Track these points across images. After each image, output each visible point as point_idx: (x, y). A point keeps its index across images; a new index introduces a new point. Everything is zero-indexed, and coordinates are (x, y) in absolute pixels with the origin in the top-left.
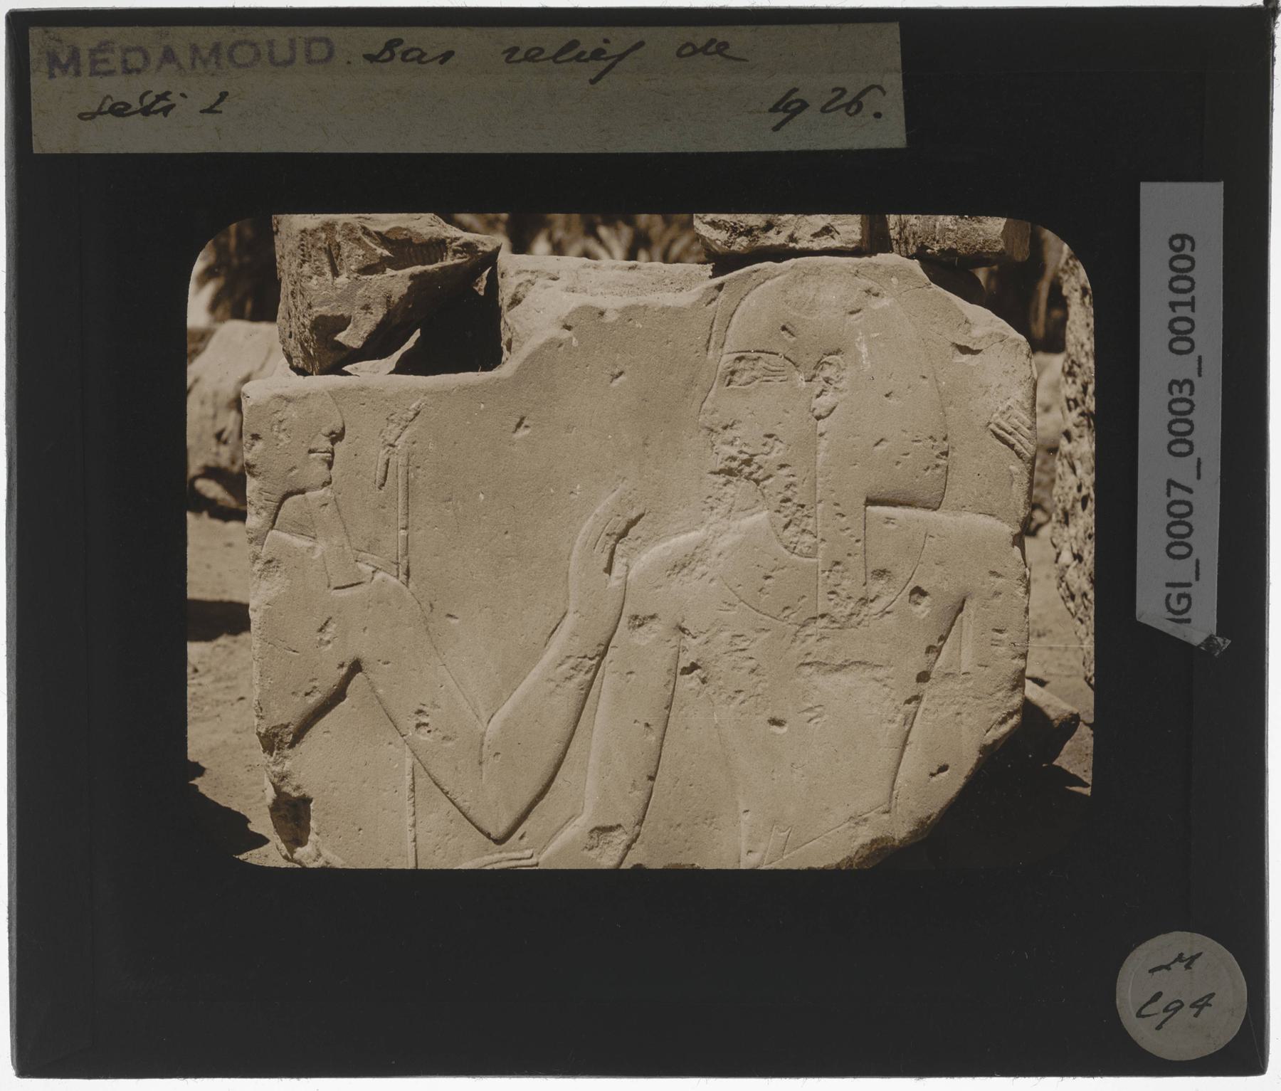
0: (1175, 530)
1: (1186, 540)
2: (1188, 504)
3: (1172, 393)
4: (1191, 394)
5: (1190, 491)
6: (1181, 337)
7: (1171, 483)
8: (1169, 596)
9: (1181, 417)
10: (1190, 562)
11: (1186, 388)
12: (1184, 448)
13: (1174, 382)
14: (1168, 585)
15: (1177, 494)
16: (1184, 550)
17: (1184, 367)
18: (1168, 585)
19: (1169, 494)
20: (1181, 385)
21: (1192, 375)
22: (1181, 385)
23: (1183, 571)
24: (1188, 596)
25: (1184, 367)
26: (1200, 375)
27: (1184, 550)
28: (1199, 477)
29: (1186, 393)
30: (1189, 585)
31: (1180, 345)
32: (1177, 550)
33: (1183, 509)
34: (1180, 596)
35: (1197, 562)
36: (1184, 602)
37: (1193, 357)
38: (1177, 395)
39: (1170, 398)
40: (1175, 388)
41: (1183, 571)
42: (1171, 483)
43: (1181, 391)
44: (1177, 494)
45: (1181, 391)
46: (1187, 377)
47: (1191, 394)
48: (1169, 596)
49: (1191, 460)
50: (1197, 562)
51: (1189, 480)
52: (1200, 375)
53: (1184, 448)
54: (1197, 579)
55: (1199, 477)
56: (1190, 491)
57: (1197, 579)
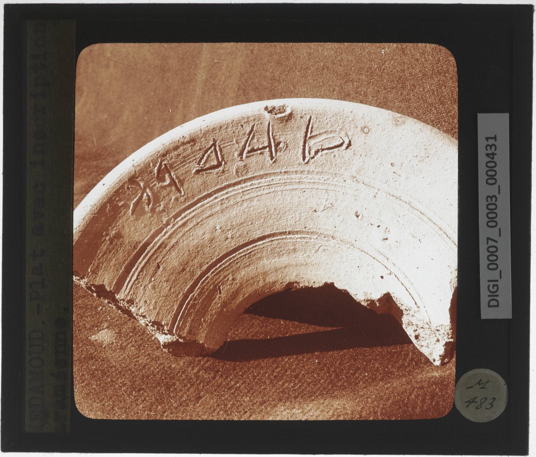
0: (491, 258)
1: (496, 262)
2: (496, 247)
3: (487, 201)
4: (496, 201)
5: (496, 242)
6: (492, 178)
7: (488, 239)
8: (489, 286)
9: (492, 211)
10: (497, 272)
11: (494, 199)
12: (493, 224)
13: (488, 197)
14: (489, 281)
15: (491, 243)
16: (495, 266)
17: (493, 190)
18: (489, 281)
19: (488, 244)
20: (491, 198)
21: (496, 194)
22: (491, 198)
23: (495, 275)
24: (497, 285)
25: (493, 190)
26: (499, 193)
27: (495, 266)
28: (500, 236)
29: (493, 201)
30: (497, 281)
31: (490, 181)
32: (491, 267)
33: (493, 249)
34: (494, 286)
35: (500, 271)
36: (496, 288)
37: (496, 186)
38: (490, 202)
39: (488, 203)
40: (489, 199)
41: (495, 275)
42: (488, 239)
43: (491, 200)
44: (491, 243)
45: (491, 200)
46: (494, 194)
47: (496, 201)
48: (489, 286)
49: (496, 229)
50: (500, 271)
51: (495, 237)
52: (499, 193)
53: (493, 224)
54: (501, 278)
55: (500, 236)
56: (496, 242)
57: (501, 278)
